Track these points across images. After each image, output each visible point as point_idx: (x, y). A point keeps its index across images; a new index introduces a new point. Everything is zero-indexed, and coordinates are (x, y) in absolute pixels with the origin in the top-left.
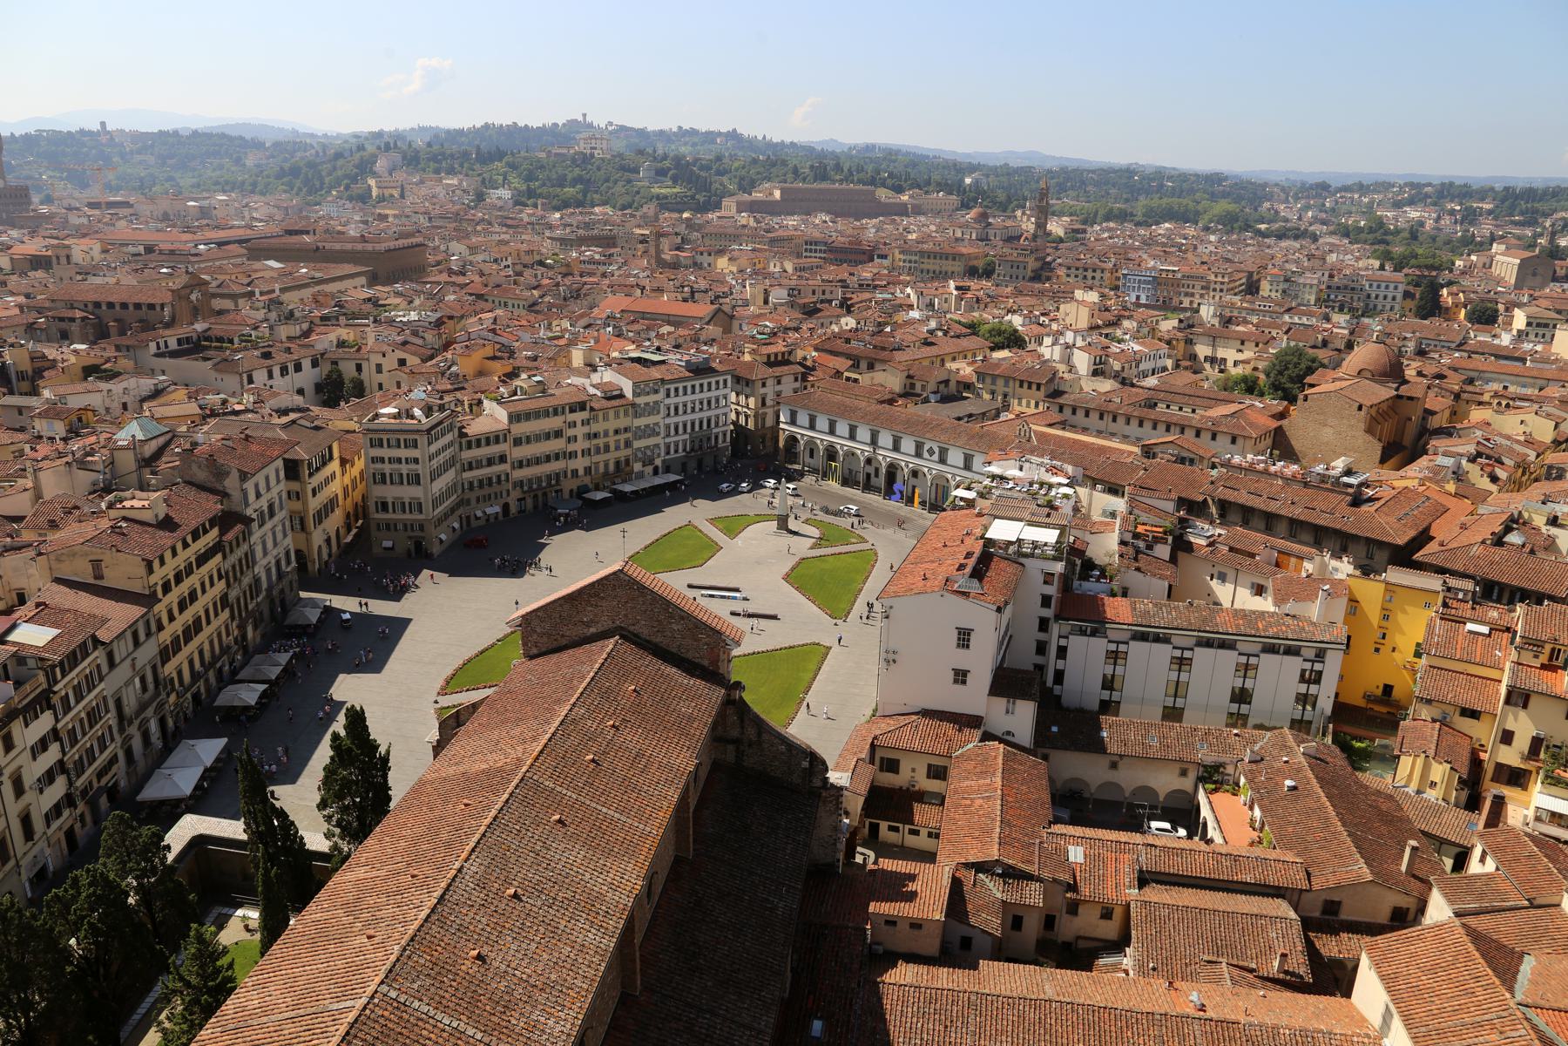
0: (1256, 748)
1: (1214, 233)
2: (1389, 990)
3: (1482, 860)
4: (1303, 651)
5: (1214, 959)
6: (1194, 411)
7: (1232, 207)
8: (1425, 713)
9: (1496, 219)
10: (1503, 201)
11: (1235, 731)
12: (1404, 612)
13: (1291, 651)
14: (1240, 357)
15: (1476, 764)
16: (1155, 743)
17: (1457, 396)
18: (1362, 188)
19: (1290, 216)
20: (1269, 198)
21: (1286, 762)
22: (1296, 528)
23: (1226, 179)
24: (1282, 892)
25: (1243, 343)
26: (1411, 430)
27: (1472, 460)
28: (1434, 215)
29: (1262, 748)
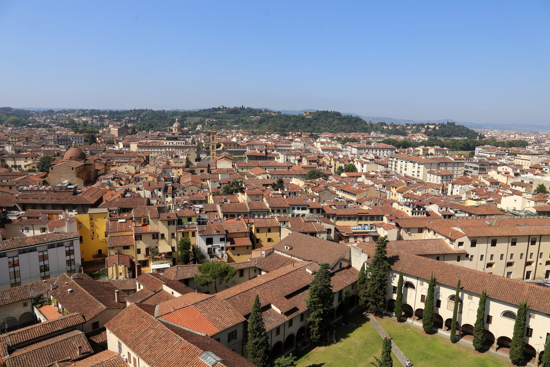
0: (54, 284)
1: (10, 127)
2: (117, 336)
3: (139, 288)
4: (64, 244)
5: (52, 363)
6: (8, 181)
7: (16, 118)
8: (112, 252)
9: (109, 119)
10: (110, 114)
11: (44, 281)
12: (97, 221)
13: (60, 245)
14: (26, 164)
15: (132, 263)
16: (8, 297)
17: (106, 165)
18: (65, 112)
19: (41, 121)
20: (32, 115)
21: (67, 284)
22: (55, 206)
23: (12, 109)
24: (75, 327)
25: (26, 158)
26: (92, 175)
27: (113, 180)
28: (91, 119)
29: (57, 283)
